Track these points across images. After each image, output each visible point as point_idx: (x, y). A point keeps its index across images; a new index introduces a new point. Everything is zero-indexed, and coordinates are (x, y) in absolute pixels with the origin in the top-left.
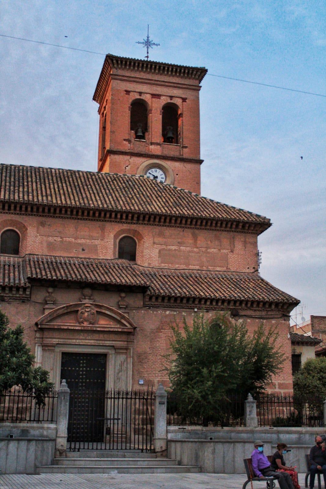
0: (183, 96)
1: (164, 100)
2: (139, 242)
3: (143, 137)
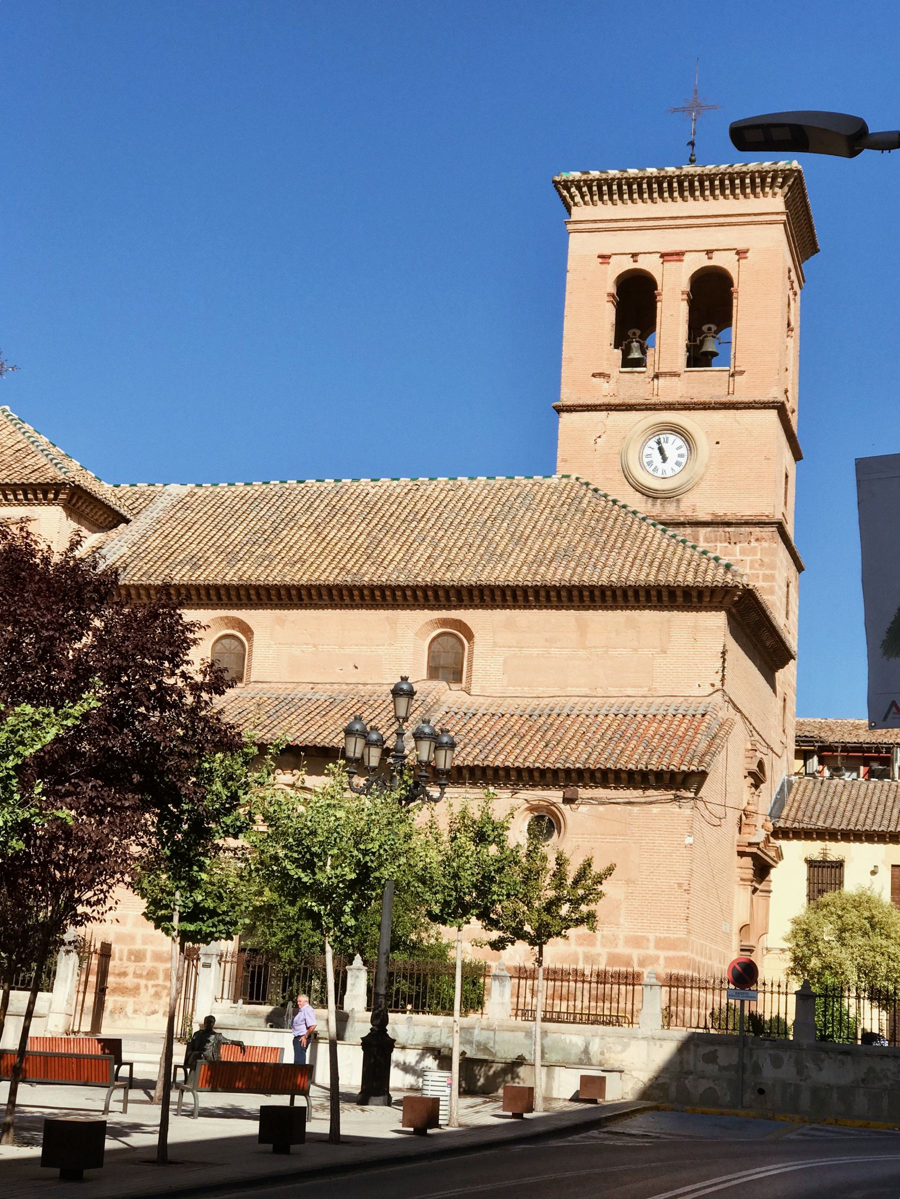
0: (741, 246)
1: (694, 263)
2: (469, 642)
3: (640, 363)
